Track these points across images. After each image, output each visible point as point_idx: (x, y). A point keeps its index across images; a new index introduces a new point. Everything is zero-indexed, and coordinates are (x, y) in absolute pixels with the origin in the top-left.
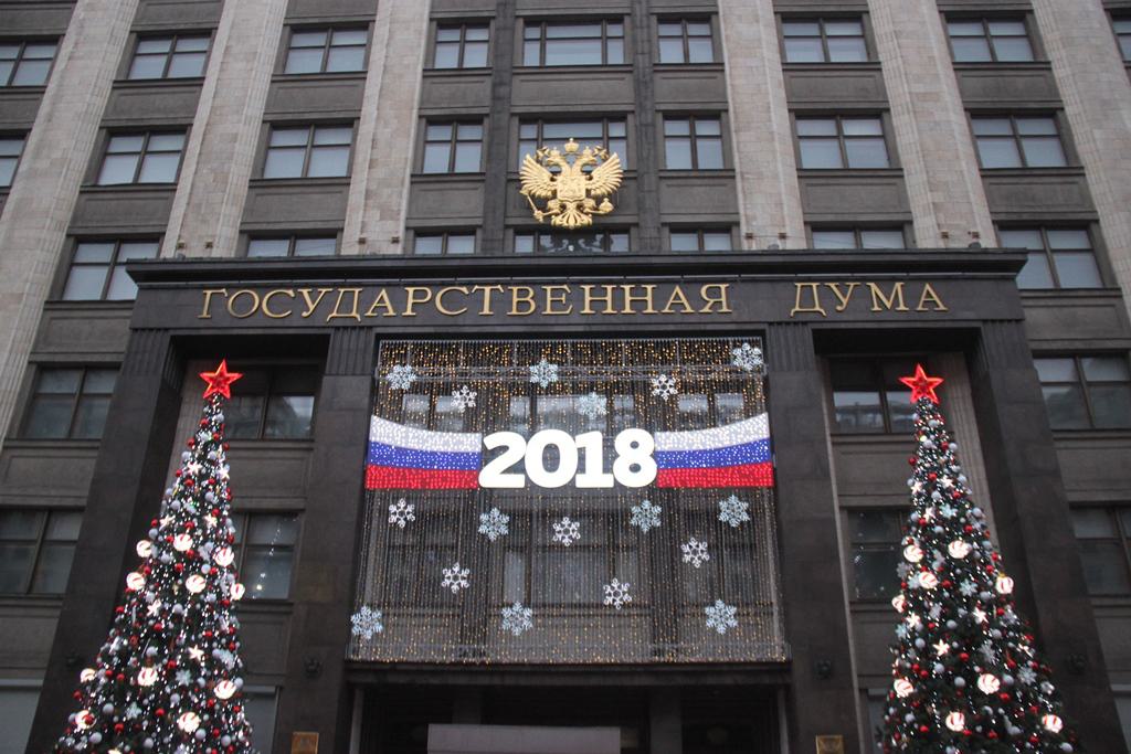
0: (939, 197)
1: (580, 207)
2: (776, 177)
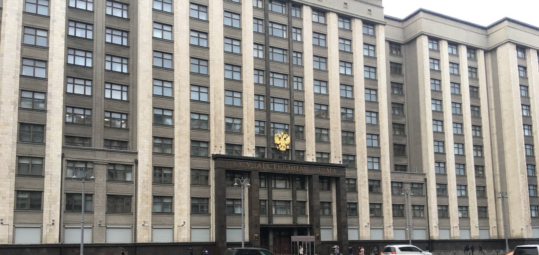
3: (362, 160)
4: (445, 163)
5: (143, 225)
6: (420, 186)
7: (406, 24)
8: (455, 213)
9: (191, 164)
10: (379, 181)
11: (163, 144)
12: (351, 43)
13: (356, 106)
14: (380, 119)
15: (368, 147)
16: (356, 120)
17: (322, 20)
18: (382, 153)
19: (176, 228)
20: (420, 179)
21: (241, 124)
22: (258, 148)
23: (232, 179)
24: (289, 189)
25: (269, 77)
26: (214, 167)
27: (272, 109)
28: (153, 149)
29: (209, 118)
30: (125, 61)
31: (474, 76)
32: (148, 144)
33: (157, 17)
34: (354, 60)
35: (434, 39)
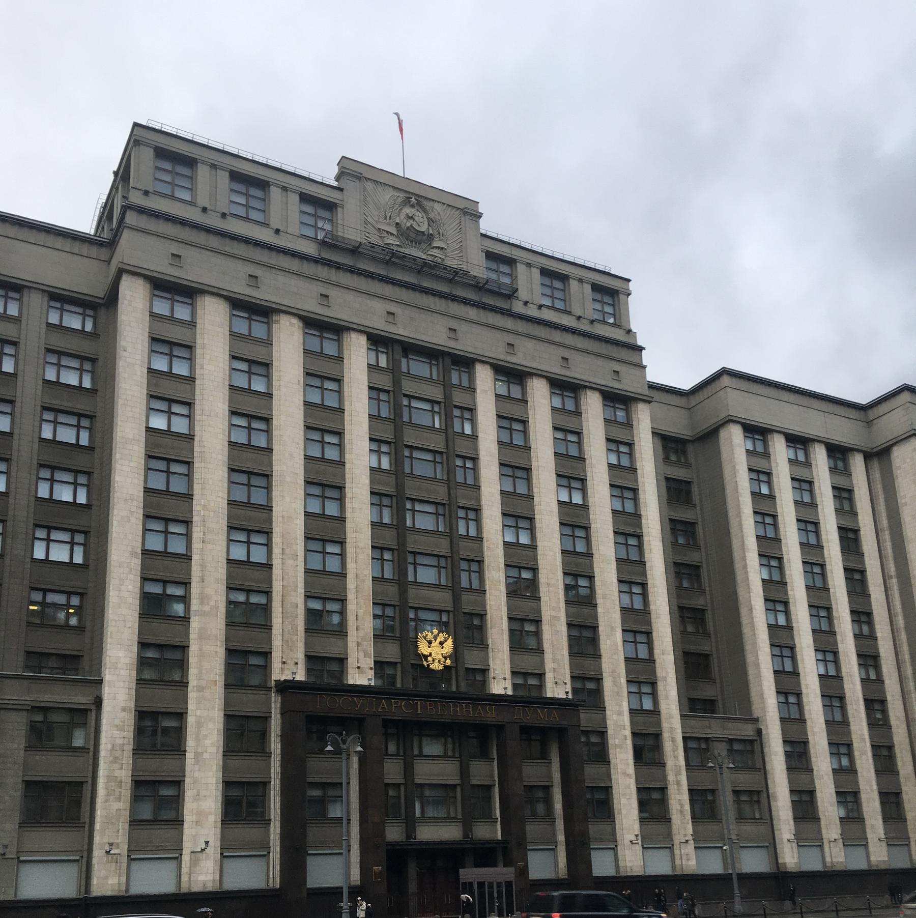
0: (556, 666)
3: (616, 689)
4: (799, 695)
5: (108, 852)
6: (749, 748)
7: (694, 400)
8: (830, 808)
9: (227, 703)
10: (657, 736)
11: (163, 660)
12: (579, 438)
13: (597, 571)
14: (651, 599)
16: (600, 601)
17: (516, 391)
18: (660, 673)
19: (186, 857)
20: (747, 731)
21: (343, 613)
22: (379, 666)
23: (322, 739)
24: (453, 757)
25: (405, 510)
26: (278, 711)
27: (411, 578)
28: (140, 670)
29: (269, 600)
30: (82, 479)
31: (847, 506)
32: (128, 661)
34: (589, 474)
35: (753, 430)
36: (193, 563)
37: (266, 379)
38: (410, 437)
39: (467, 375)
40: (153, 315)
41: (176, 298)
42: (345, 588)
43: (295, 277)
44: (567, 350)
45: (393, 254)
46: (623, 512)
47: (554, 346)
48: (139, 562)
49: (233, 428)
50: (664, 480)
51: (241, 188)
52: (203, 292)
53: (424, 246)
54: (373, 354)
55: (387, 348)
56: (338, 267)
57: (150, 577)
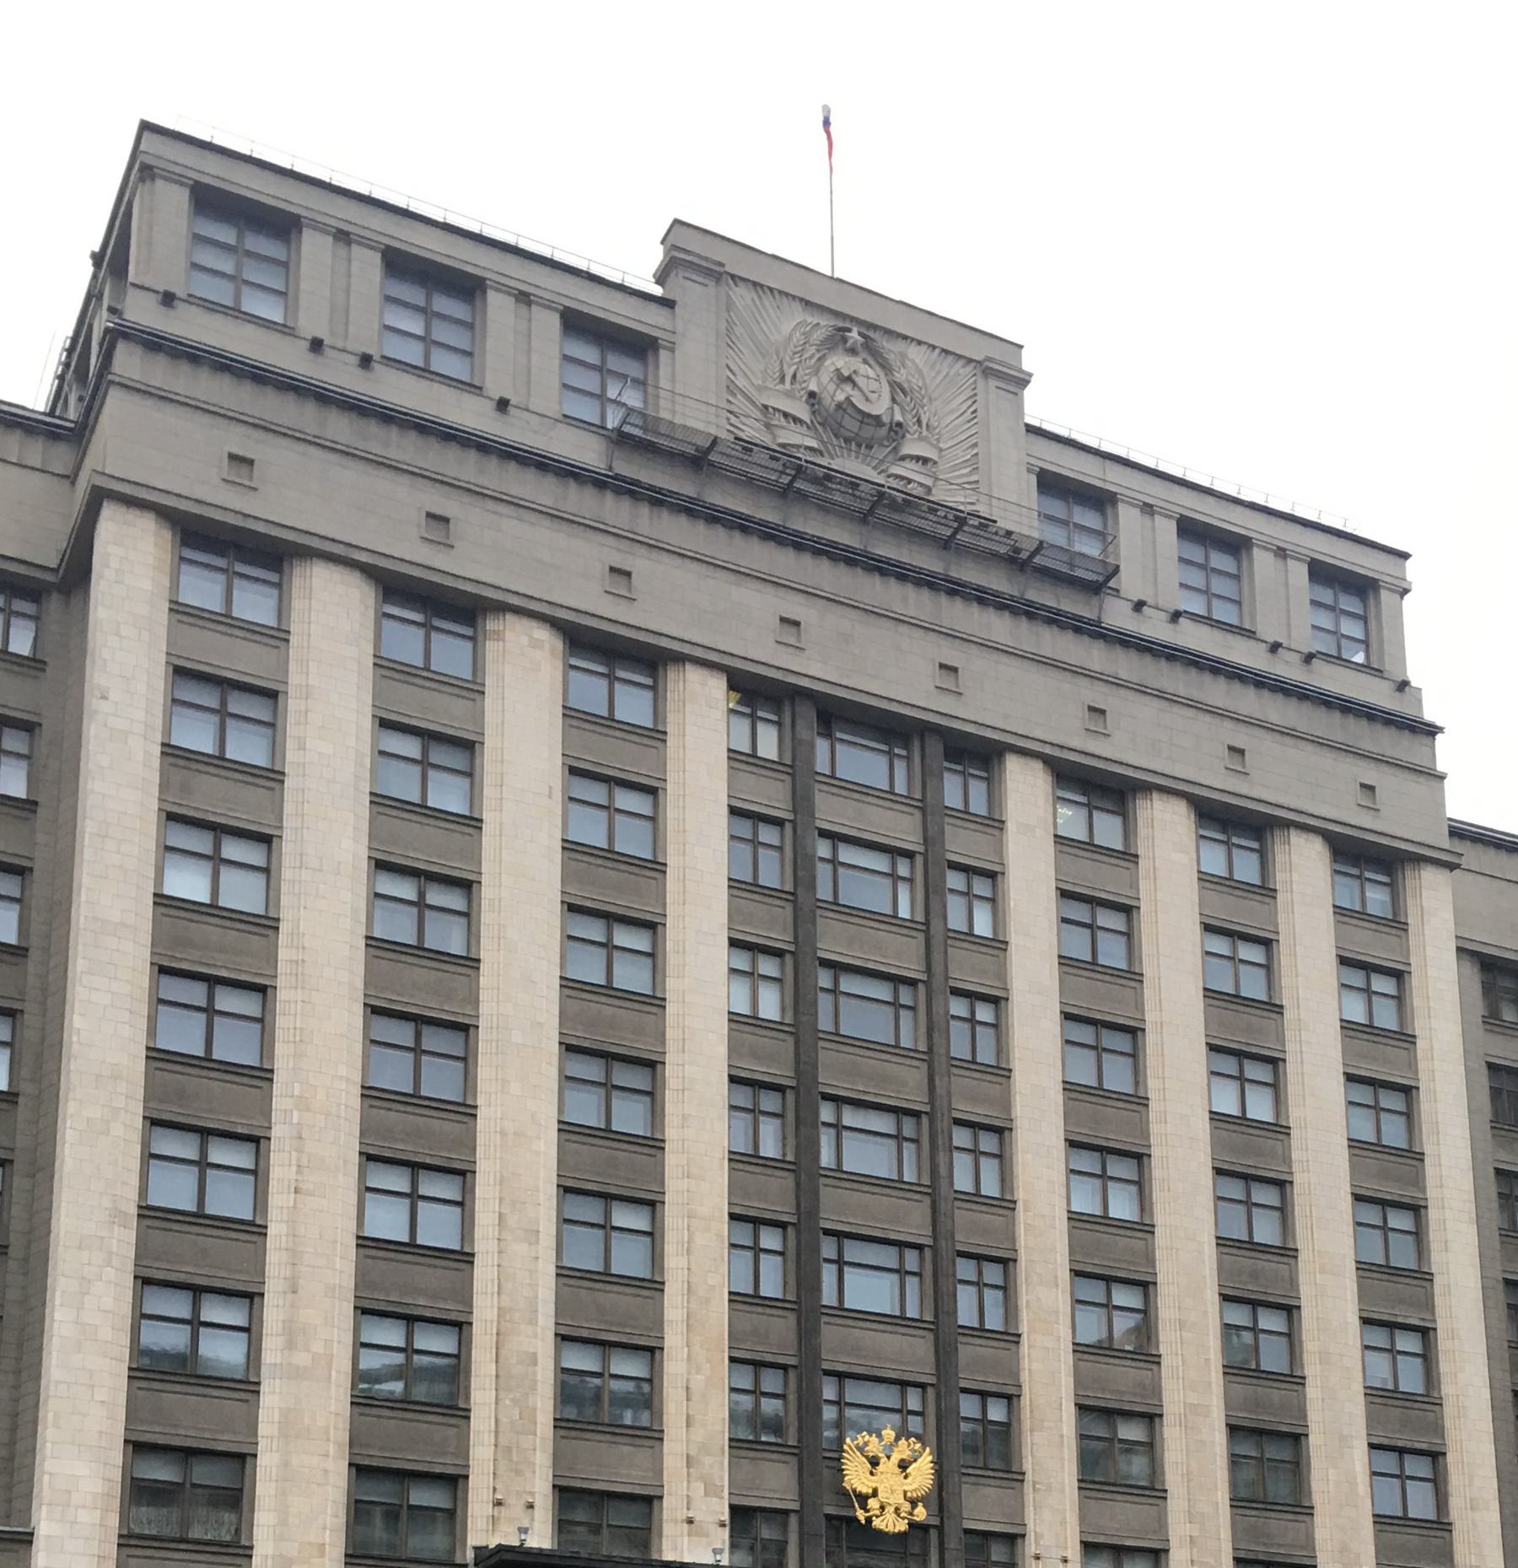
1: (897, 1510)
2: (1062, 1491)
12: (1269, 956)
14: (1444, 1366)
15: (1380, 1520)
17: (1108, 830)
22: (742, 1517)
25: (815, 1123)
27: (828, 1297)
29: (464, 1343)
32: (98, 1487)
33: (185, 789)
34: (1289, 1047)
36: (270, 1242)
37: (464, 782)
38: (834, 941)
39: (983, 786)
40: (177, 609)
41: (241, 568)
42: (659, 1323)
43: (547, 522)
44: (1243, 728)
45: (799, 469)
46: (1378, 1147)
47: (1208, 718)
48: (132, 1236)
49: (379, 902)
50: (1484, 1071)
51: (413, 294)
52: (307, 553)
53: (880, 453)
54: (743, 726)
55: (778, 711)
56: (658, 499)
57: (160, 1275)
